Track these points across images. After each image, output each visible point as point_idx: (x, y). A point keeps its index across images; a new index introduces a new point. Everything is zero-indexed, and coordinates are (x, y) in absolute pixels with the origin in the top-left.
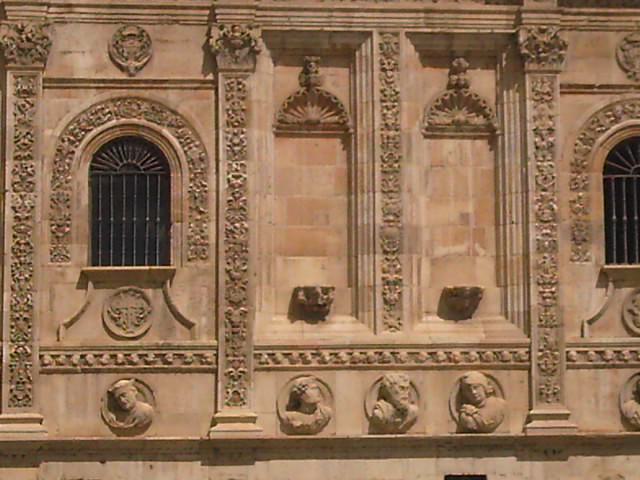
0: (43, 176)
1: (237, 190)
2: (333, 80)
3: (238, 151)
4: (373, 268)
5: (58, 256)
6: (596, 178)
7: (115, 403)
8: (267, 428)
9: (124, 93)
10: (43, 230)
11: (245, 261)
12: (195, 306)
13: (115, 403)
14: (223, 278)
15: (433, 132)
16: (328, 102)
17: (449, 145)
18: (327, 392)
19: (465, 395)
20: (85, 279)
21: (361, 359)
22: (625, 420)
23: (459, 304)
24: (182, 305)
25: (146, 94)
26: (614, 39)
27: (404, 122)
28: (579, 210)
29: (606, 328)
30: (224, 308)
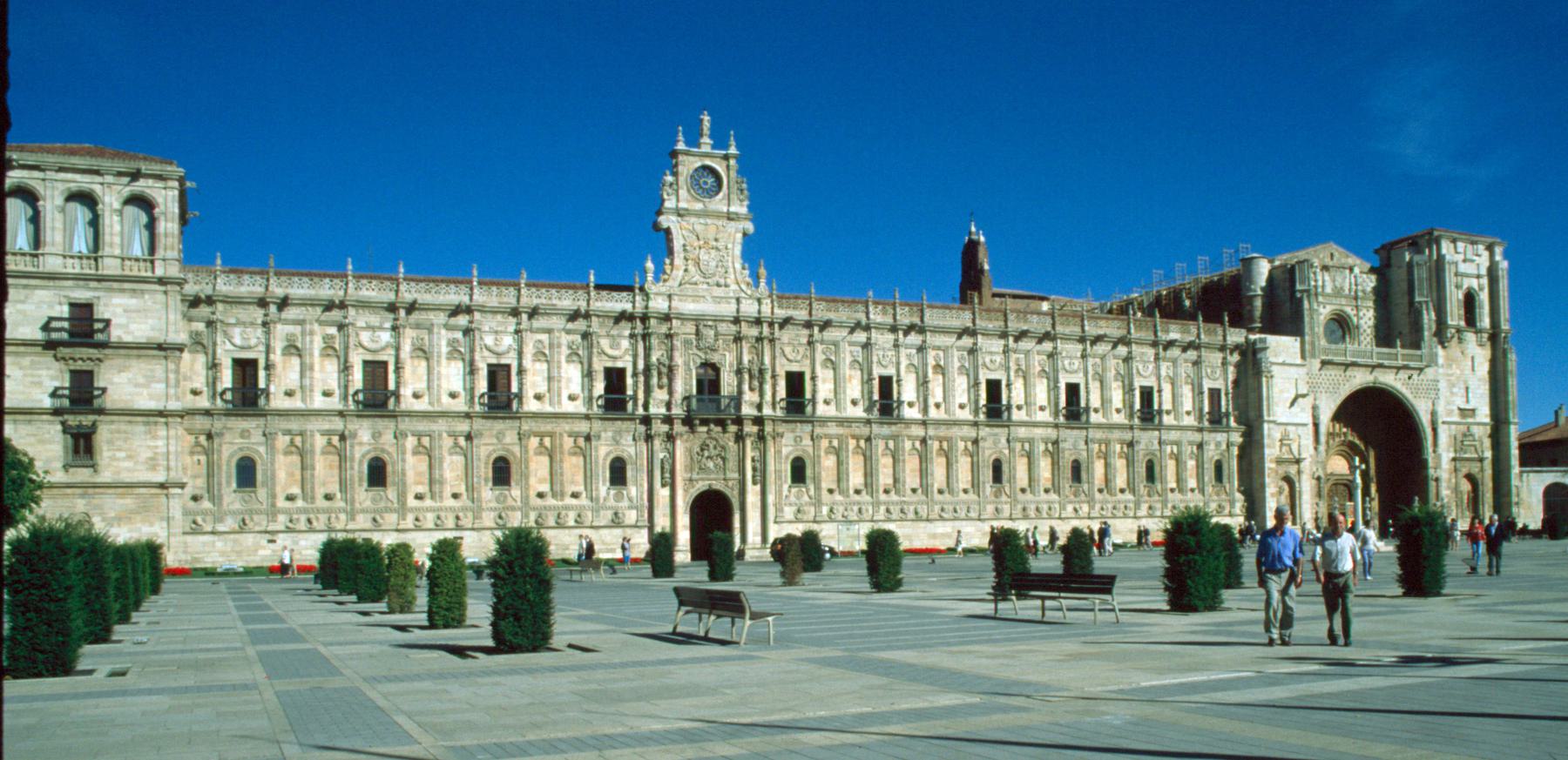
0: (356, 467)
1: (403, 470)
3: (404, 460)
4: (437, 488)
5: (360, 485)
6: (490, 466)
10: (357, 479)
13: (375, 520)
15: (451, 454)
16: (424, 447)
18: (425, 518)
20: (366, 490)
22: (497, 524)
23: (455, 496)
24: (390, 497)
26: (495, 432)
28: (486, 473)
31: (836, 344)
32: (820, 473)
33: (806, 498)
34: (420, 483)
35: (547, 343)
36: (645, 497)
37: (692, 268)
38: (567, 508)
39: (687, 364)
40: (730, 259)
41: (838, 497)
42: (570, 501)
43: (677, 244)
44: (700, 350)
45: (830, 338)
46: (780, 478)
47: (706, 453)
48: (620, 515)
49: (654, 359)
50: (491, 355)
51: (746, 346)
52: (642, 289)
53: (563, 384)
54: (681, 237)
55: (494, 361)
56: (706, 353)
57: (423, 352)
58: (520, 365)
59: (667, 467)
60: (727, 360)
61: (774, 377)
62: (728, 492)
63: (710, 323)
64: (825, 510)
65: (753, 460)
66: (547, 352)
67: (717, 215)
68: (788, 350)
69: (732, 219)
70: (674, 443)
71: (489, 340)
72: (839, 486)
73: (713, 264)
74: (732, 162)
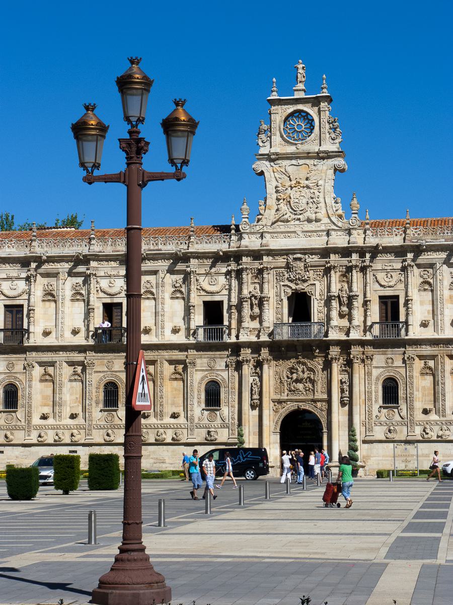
2: (50, 370)
3: (30, 387)
6: (102, 390)
7: (6, 437)
8: (35, 441)
9: (9, 375)
11: (31, 408)
12: (22, 417)
13: (6, 437)
14: (27, 411)
15: (71, 381)
16: (50, 375)
17: (74, 383)
18: (46, 434)
19: (72, 435)
21: (53, 428)
25: (13, 375)
27: (63, 379)
28: (97, 397)
29: (102, 421)
30: (27, 417)
31: (432, 266)
32: (412, 394)
33: (397, 418)
34: (45, 405)
35: (154, 283)
36: (236, 417)
37: (284, 207)
38: (166, 427)
39: (278, 295)
40: (321, 195)
41: (433, 417)
42: (168, 420)
43: (271, 189)
44: (291, 281)
45: (425, 262)
46: (370, 399)
47: (295, 376)
48: (212, 434)
49: (245, 292)
50: (106, 296)
51: (335, 277)
52: (237, 229)
53: (166, 318)
54: (274, 180)
55: (108, 301)
56: (297, 284)
57: (50, 296)
58: (407, 296)
59: (256, 389)
60: (317, 290)
61: (366, 303)
62: (317, 412)
63: (299, 256)
64: (418, 430)
65: (342, 383)
66: (154, 291)
67: (308, 156)
68: (381, 276)
69: (323, 158)
70: (261, 369)
71: (104, 283)
72: (435, 407)
73: (304, 201)
74: (323, 105)
